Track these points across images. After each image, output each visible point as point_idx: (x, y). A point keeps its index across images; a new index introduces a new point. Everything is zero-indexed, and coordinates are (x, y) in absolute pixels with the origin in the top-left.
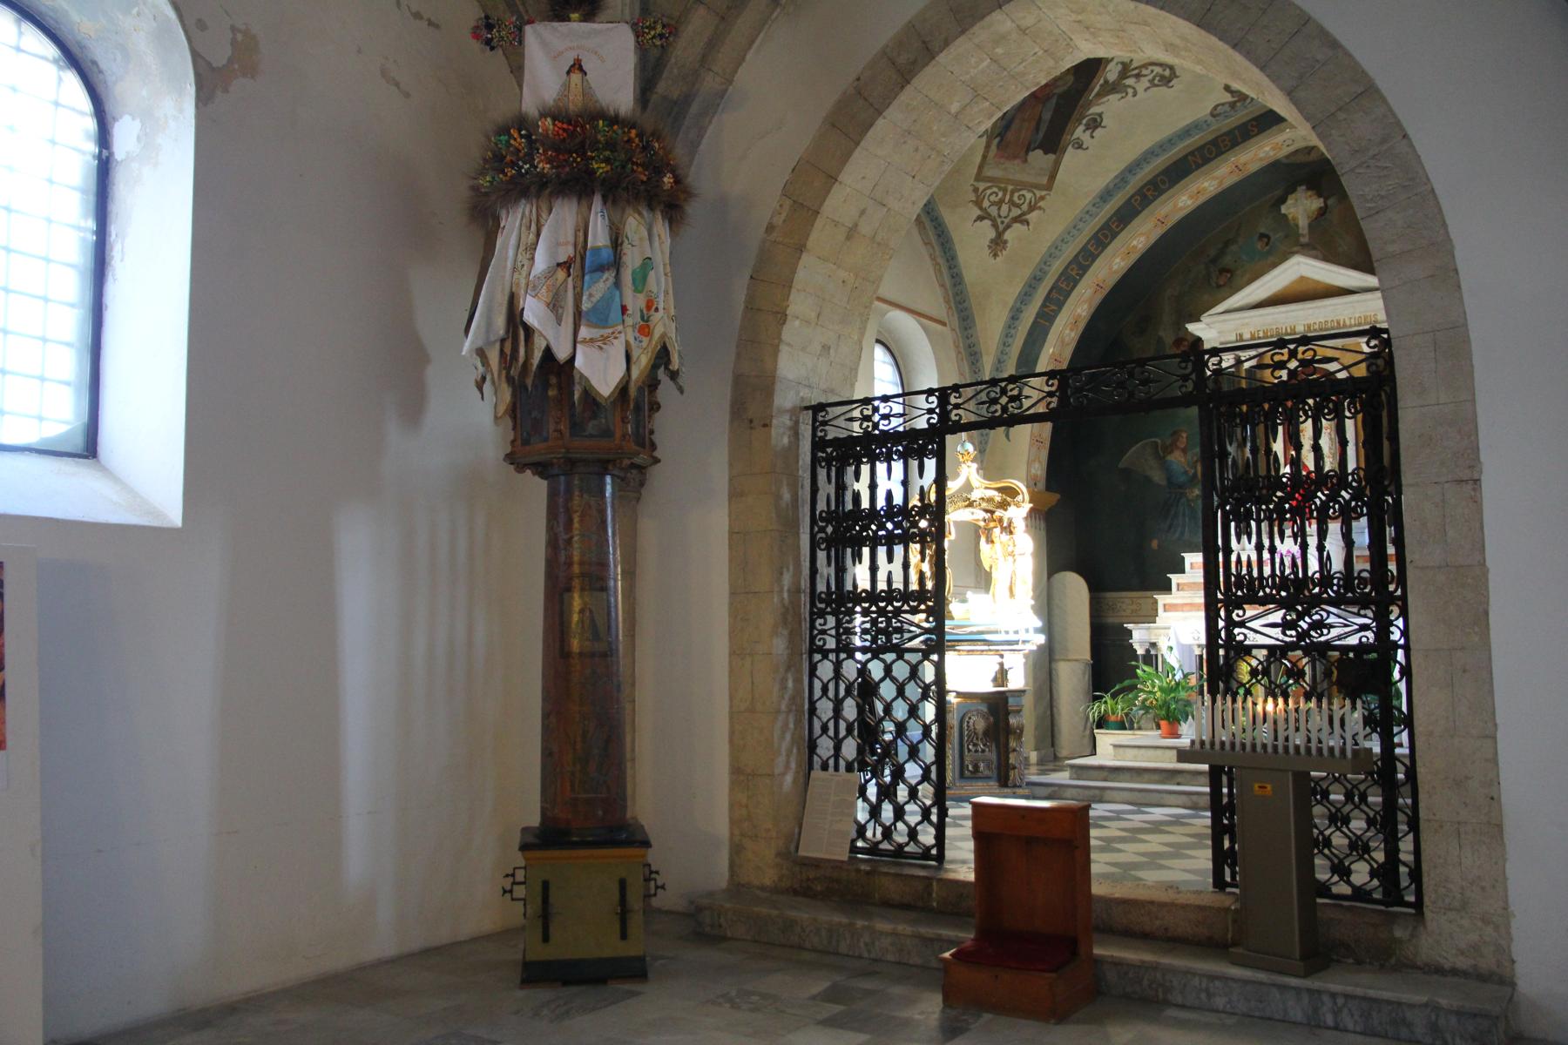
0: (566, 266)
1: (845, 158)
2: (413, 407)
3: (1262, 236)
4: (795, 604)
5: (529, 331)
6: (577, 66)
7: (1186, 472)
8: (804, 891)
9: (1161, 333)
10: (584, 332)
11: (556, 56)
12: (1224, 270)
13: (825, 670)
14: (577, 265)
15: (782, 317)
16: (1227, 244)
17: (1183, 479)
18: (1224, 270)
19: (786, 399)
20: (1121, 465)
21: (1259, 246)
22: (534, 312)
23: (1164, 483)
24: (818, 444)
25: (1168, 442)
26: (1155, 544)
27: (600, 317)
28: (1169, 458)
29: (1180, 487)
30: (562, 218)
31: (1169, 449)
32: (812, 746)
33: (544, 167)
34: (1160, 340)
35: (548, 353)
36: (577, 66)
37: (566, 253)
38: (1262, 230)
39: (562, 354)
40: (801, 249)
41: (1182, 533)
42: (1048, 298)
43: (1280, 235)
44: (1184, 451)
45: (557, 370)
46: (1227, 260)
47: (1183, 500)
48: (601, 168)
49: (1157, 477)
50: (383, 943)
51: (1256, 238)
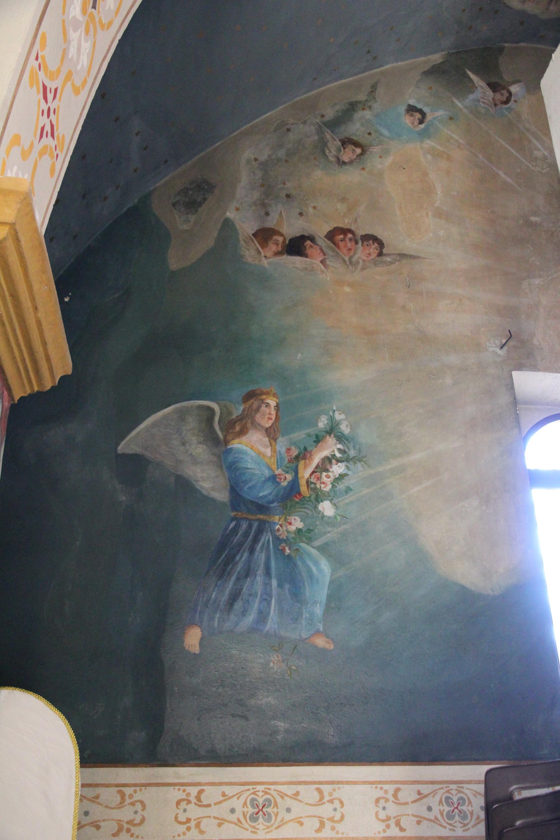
3: (411, 109)
7: (273, 478)
9: (230, 214)
12: (346, 142)
16: (353, 107)
17: (266, 492)
18: (346, 142)
20: (121, 448)
21: (407, 120)
23: (222, 496)
25: (238, 410)
26: (193, 639)
28: (236, 444)
29: (262, 508)
31: (238, 426)
34: (228, 225)
38: (412, 102)
41: (262, 617)
43: (441, 113)
44: (272, 434)
46: (355, 129)
47: (267, 537)
49: (209, 481)
51: (402, 109)
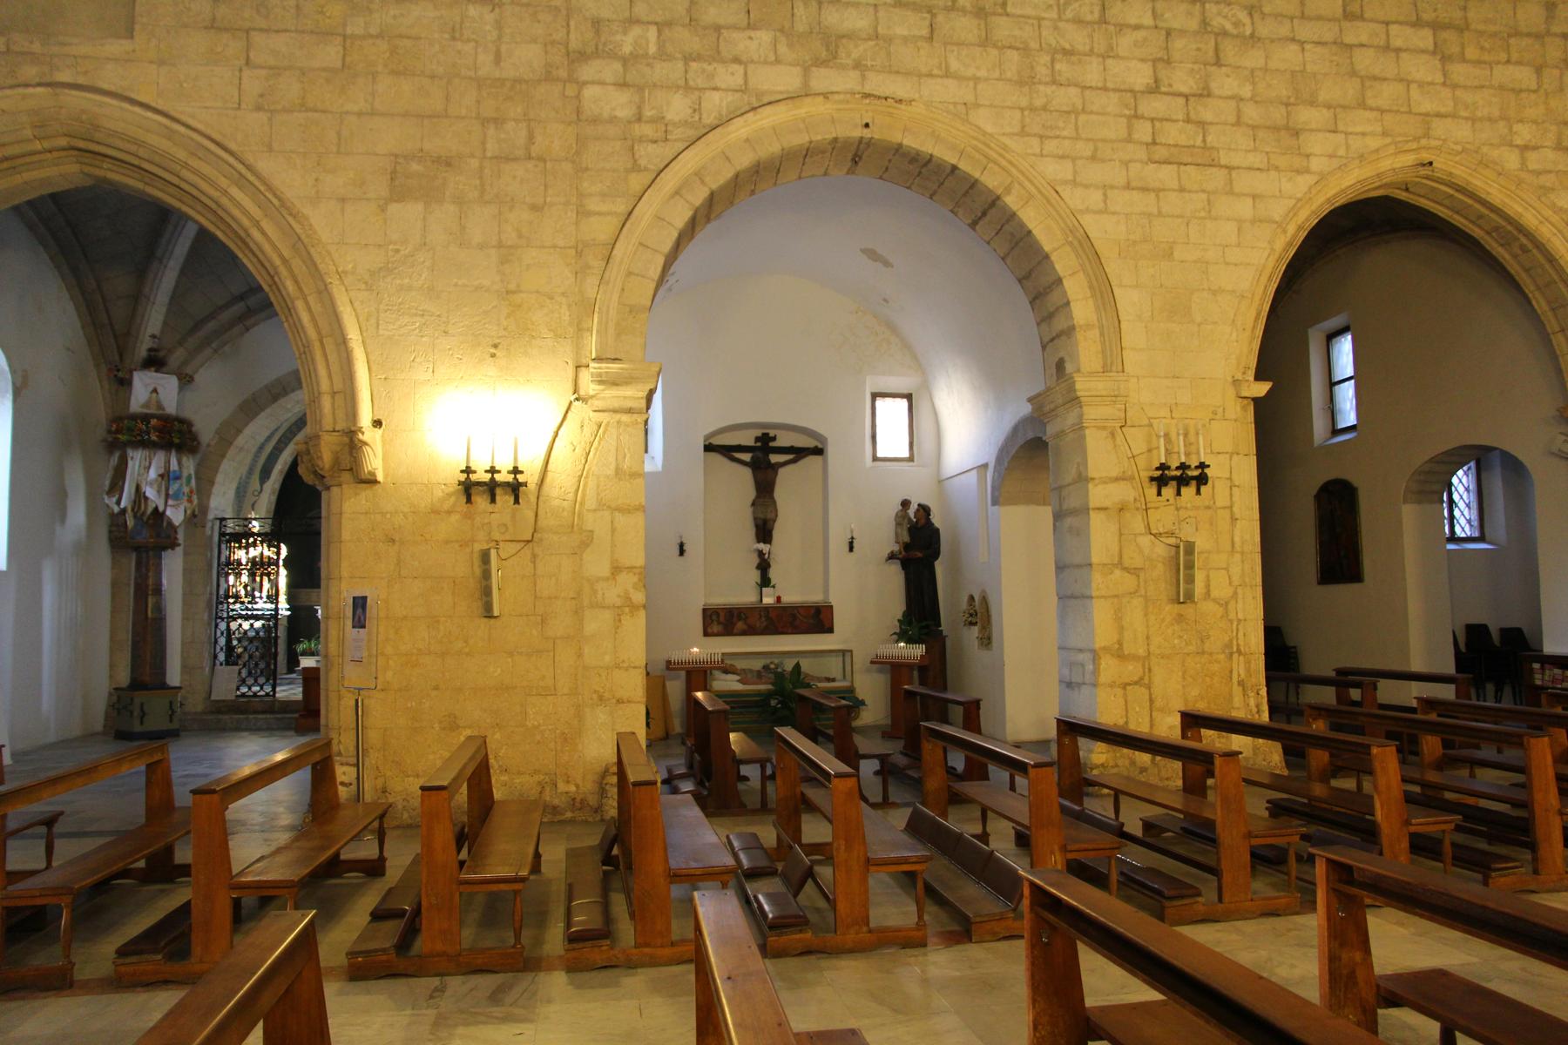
0: (162, 476)
1: (247, 424)
2: (63, 518)
4: (210, 600)
5: (146, 498)
6: (155, 391)
8: (219, 712)
10: (170, 502)
11: (146, 386)
13: (223, 626)
14: (166, 476)
15: (212, 483)
19: (211, 516)
22: (150, 493)
24: (222, 534)
27: (176, 497)
30: (159, 459)
32: (215, 657)
33: (154, 438)
35: (156, 509)
36: (155, 391)
37: (162, 471)
39: (161, 509)
40: (223, 456)
42: (280, 440)
45: (158, 515)
48: (177, 441)
50: (52, 737)
